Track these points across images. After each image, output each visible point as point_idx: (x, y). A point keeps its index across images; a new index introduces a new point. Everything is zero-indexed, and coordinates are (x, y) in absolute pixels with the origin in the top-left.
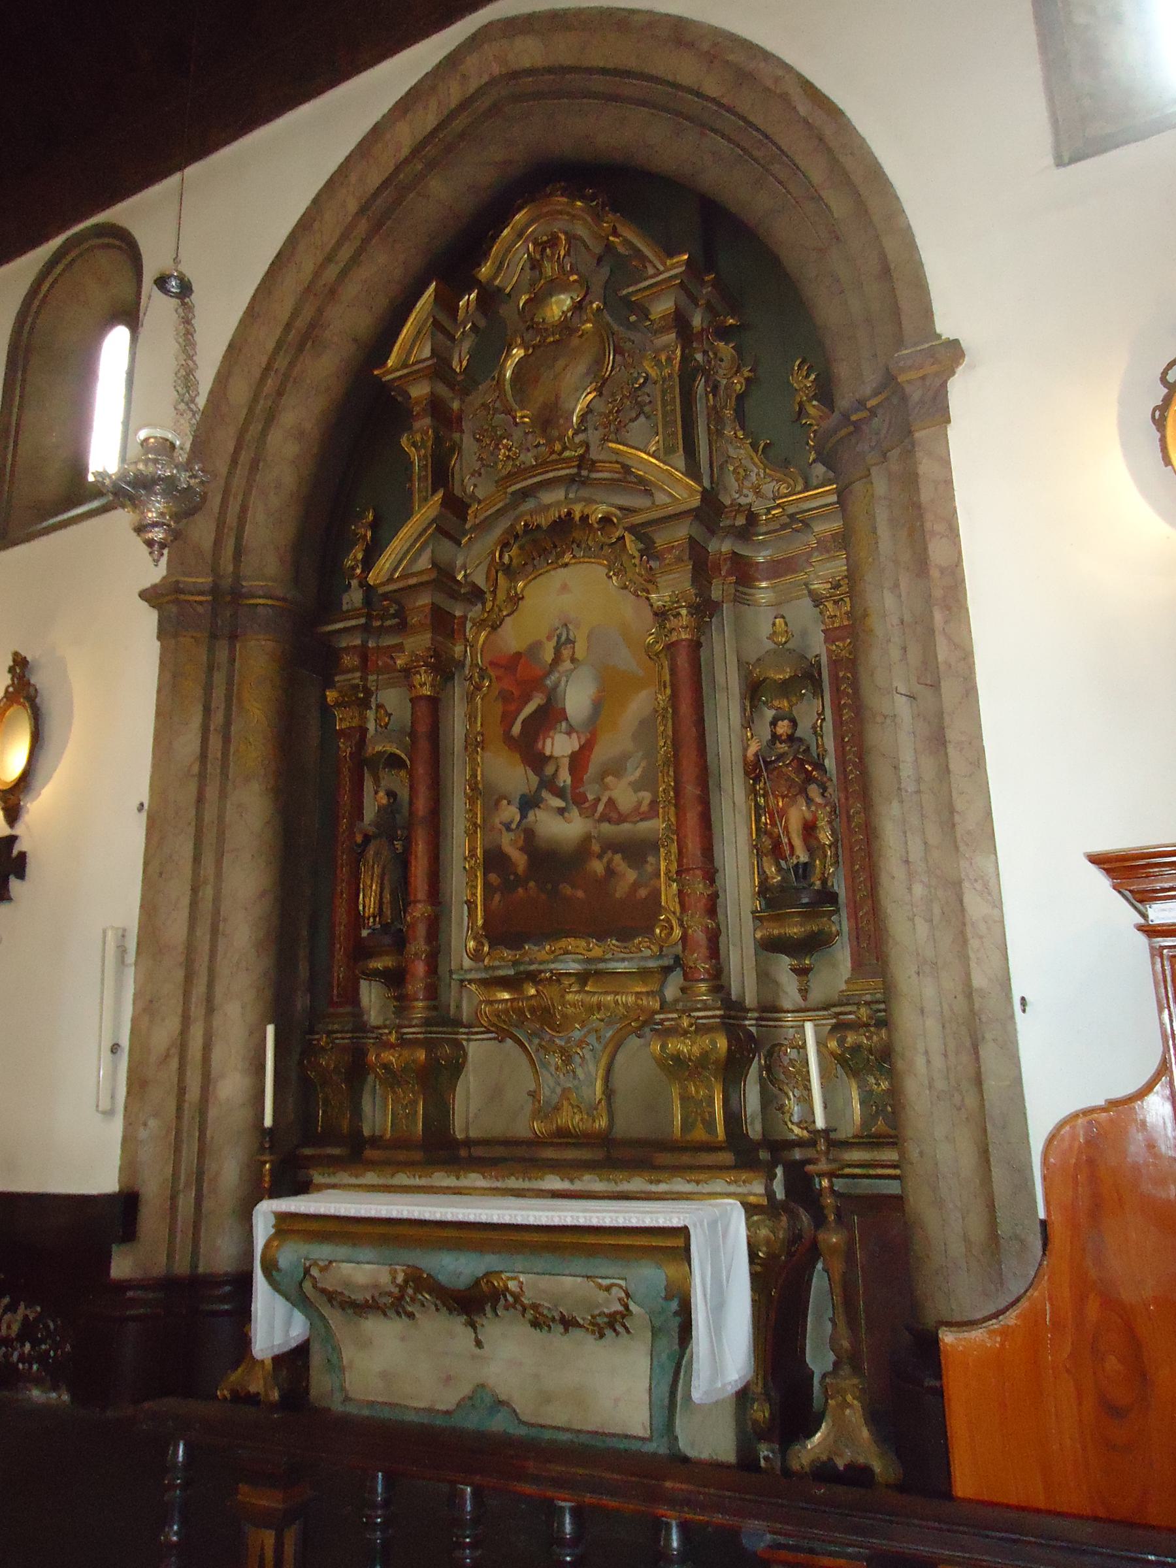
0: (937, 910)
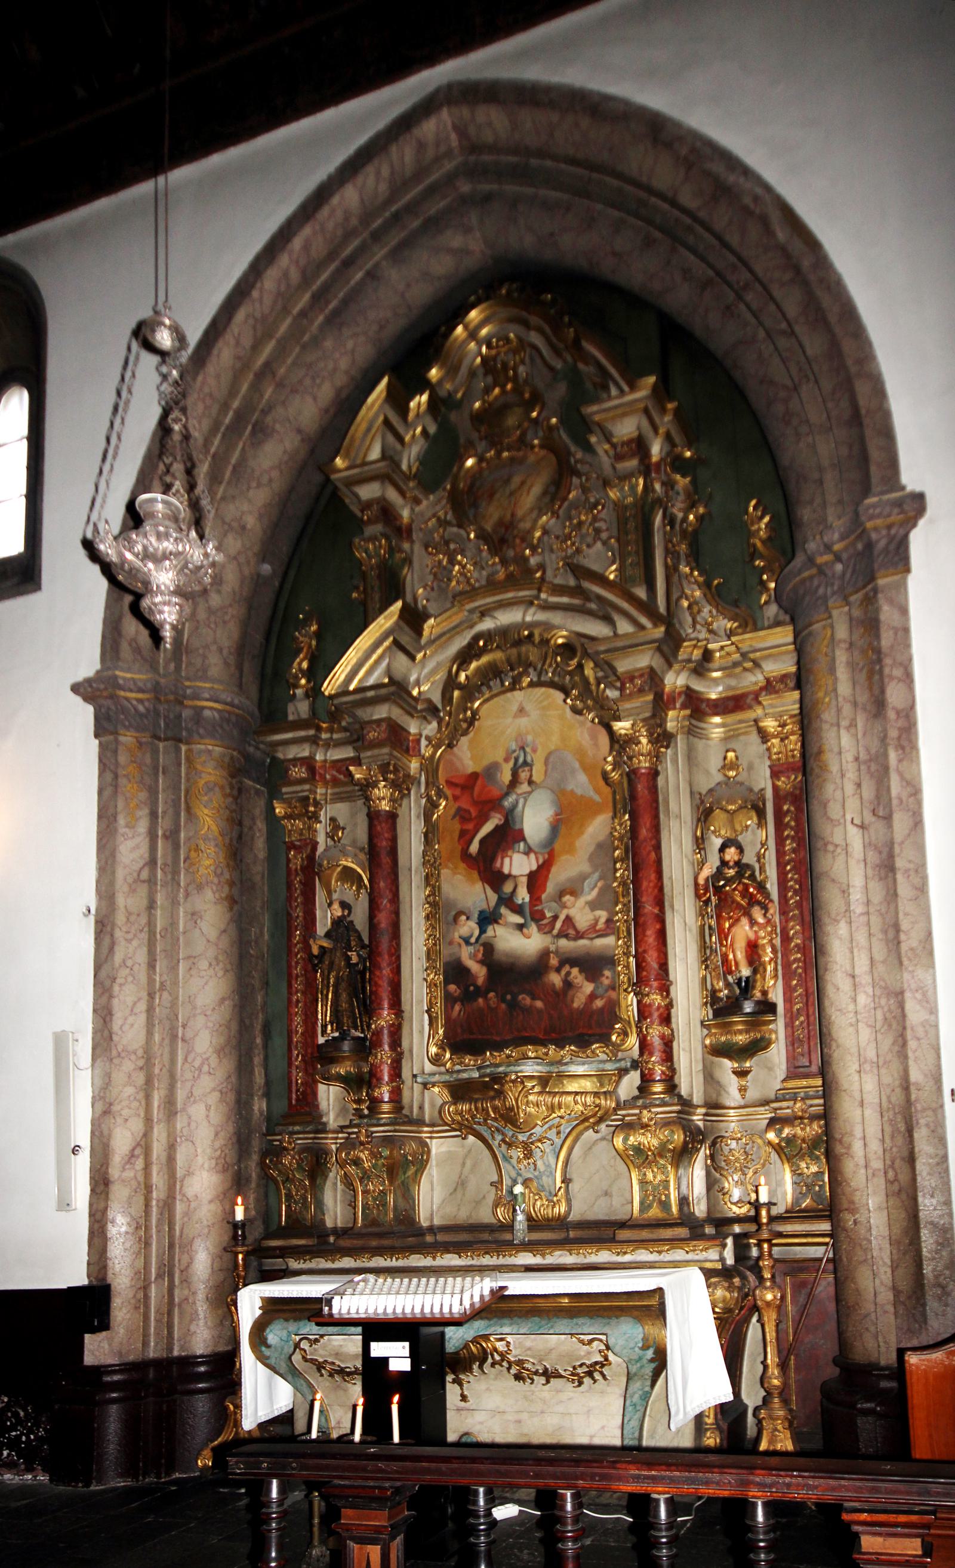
0: (880, 1016)
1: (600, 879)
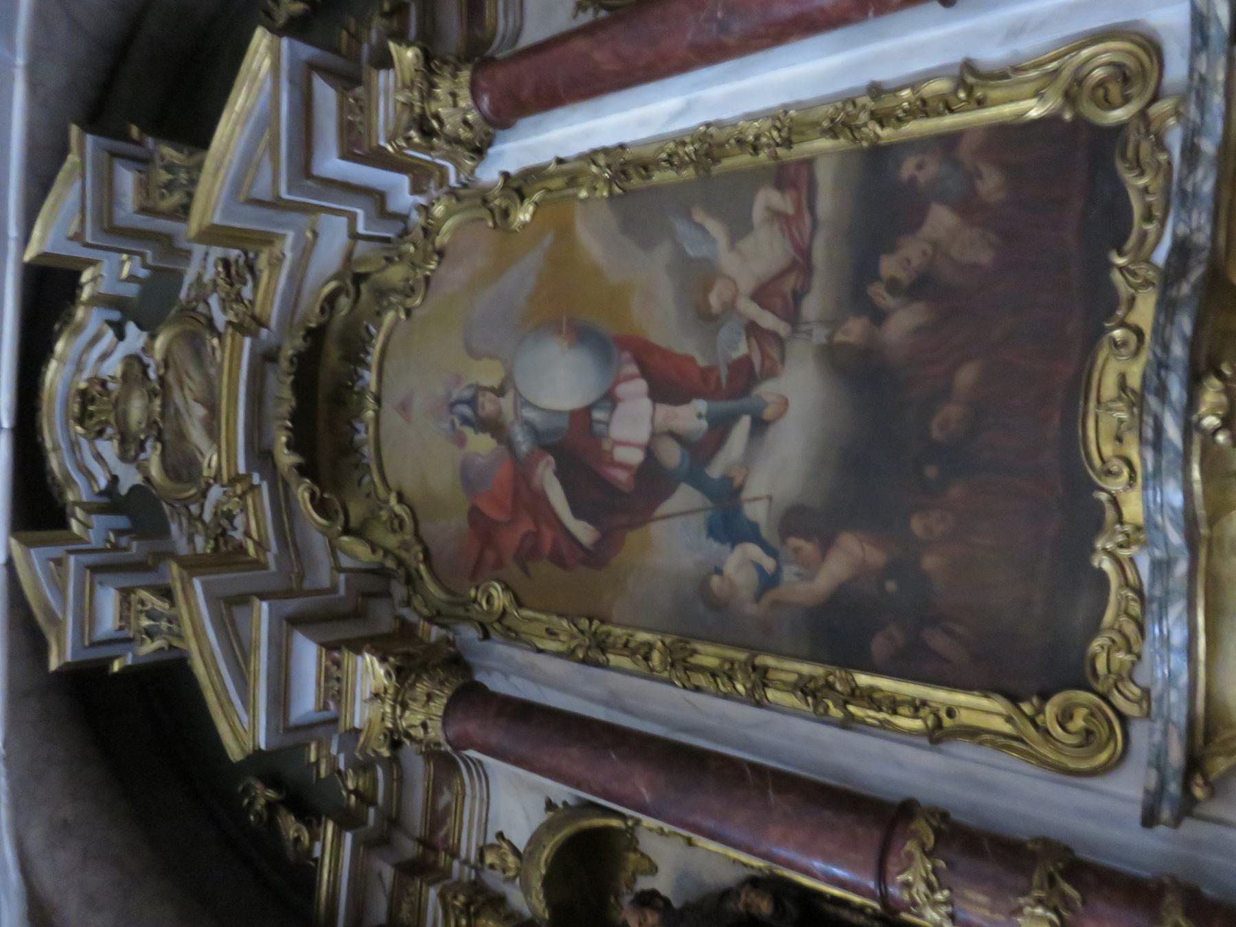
1: (688, 216)
